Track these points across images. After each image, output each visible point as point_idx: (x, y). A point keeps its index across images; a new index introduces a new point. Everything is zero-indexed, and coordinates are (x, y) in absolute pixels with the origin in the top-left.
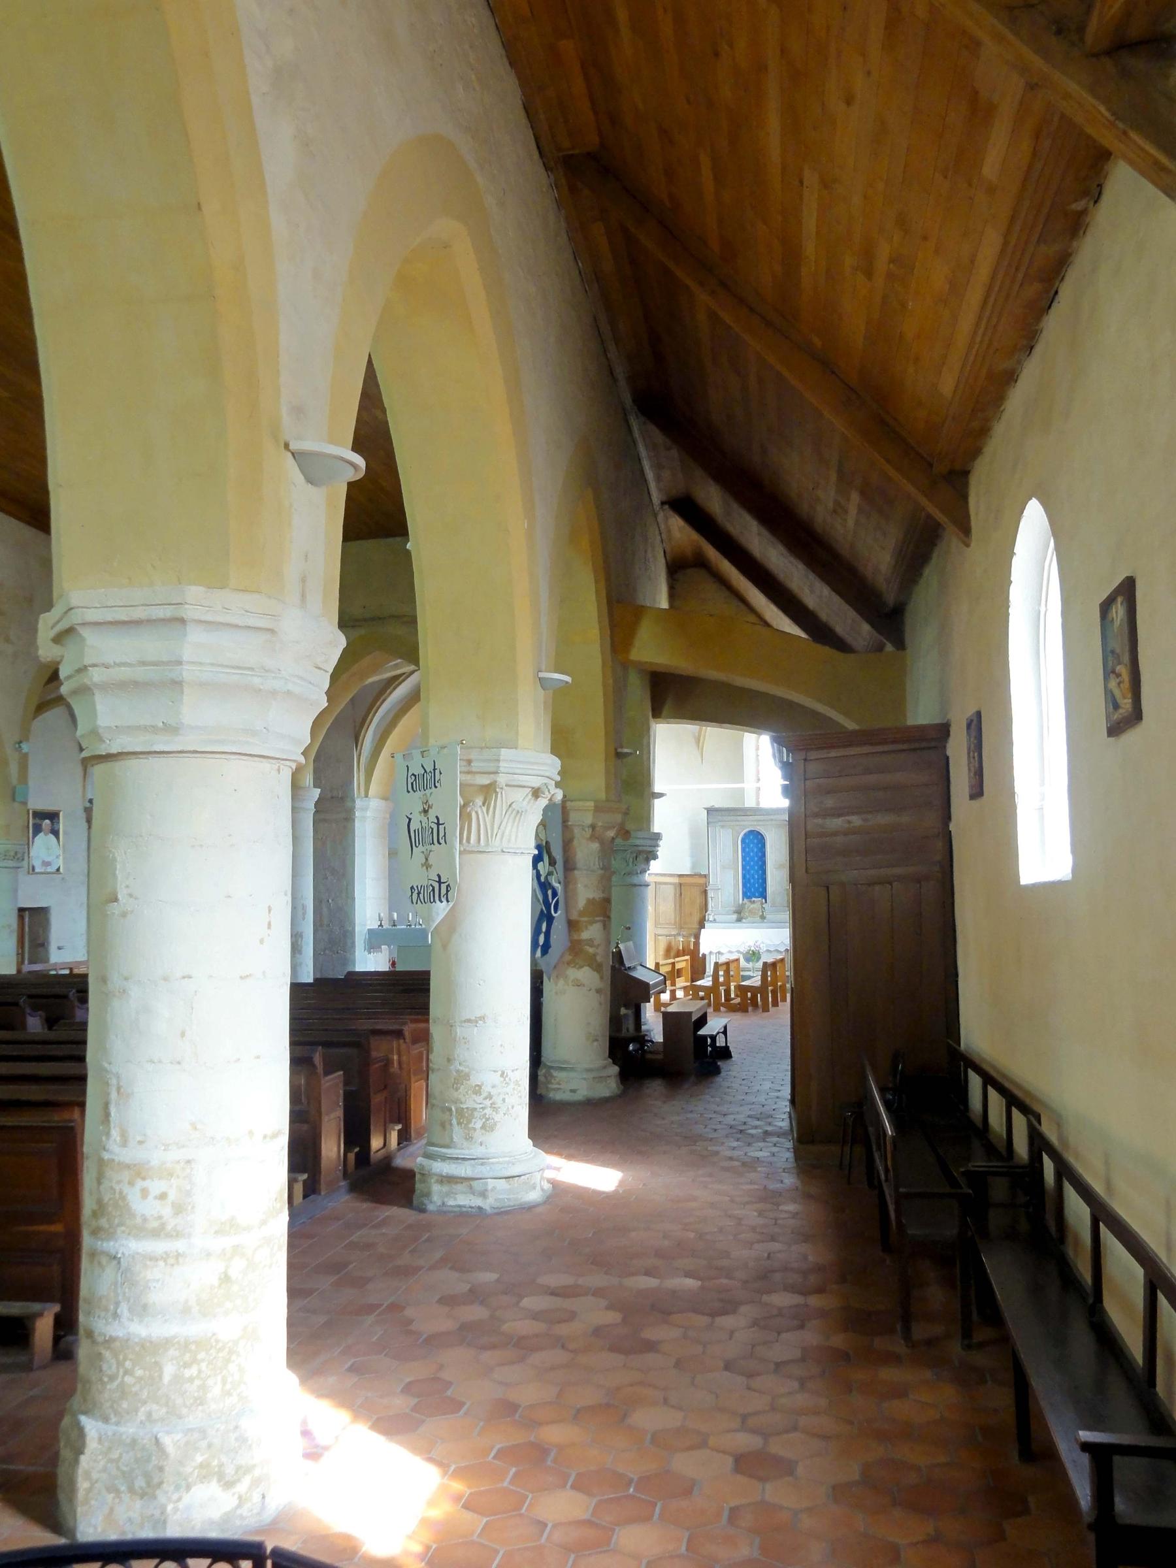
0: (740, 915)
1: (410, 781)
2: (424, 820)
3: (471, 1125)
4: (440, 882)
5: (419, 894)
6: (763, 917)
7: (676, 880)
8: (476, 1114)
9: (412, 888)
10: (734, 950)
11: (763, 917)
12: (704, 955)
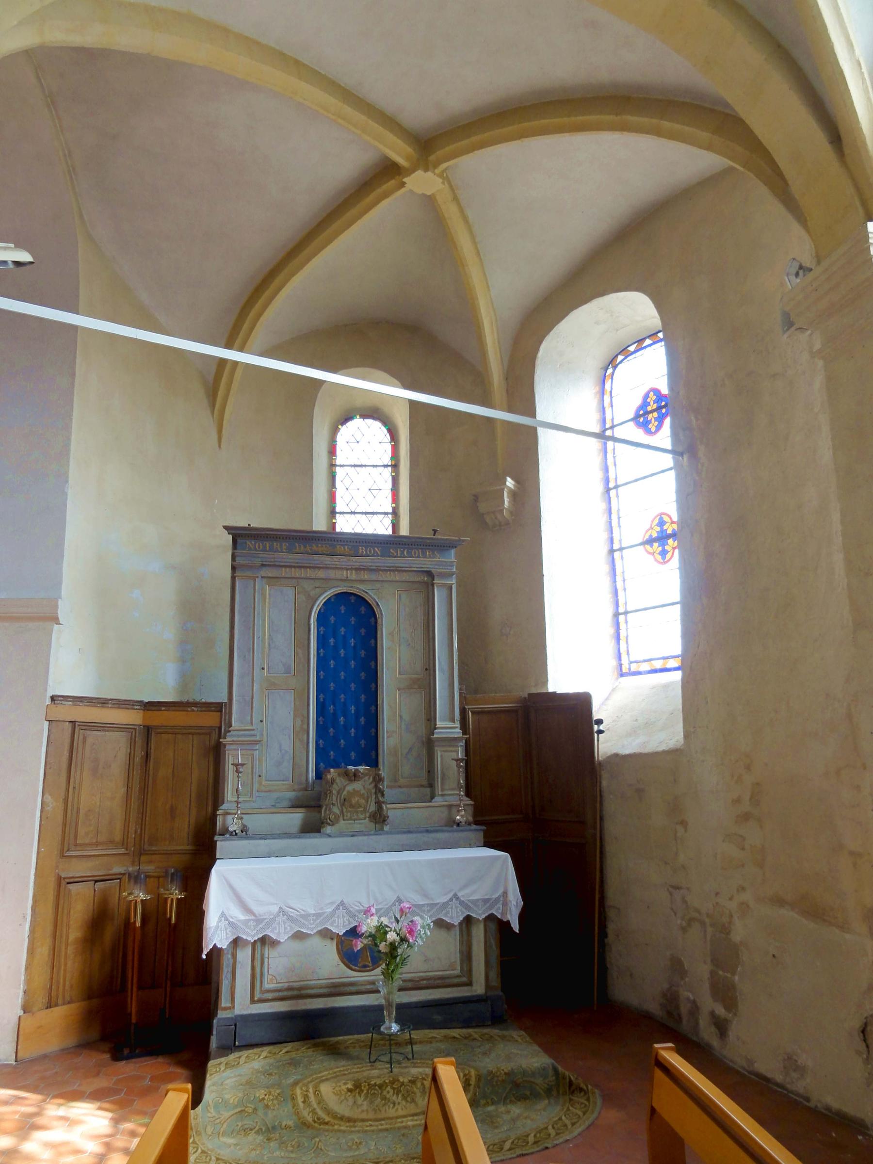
0: (315, 814)
6: (379, 818)
7: (134, 718)
10: (311, 929)
11: (379, 818)
12: (216, 951)
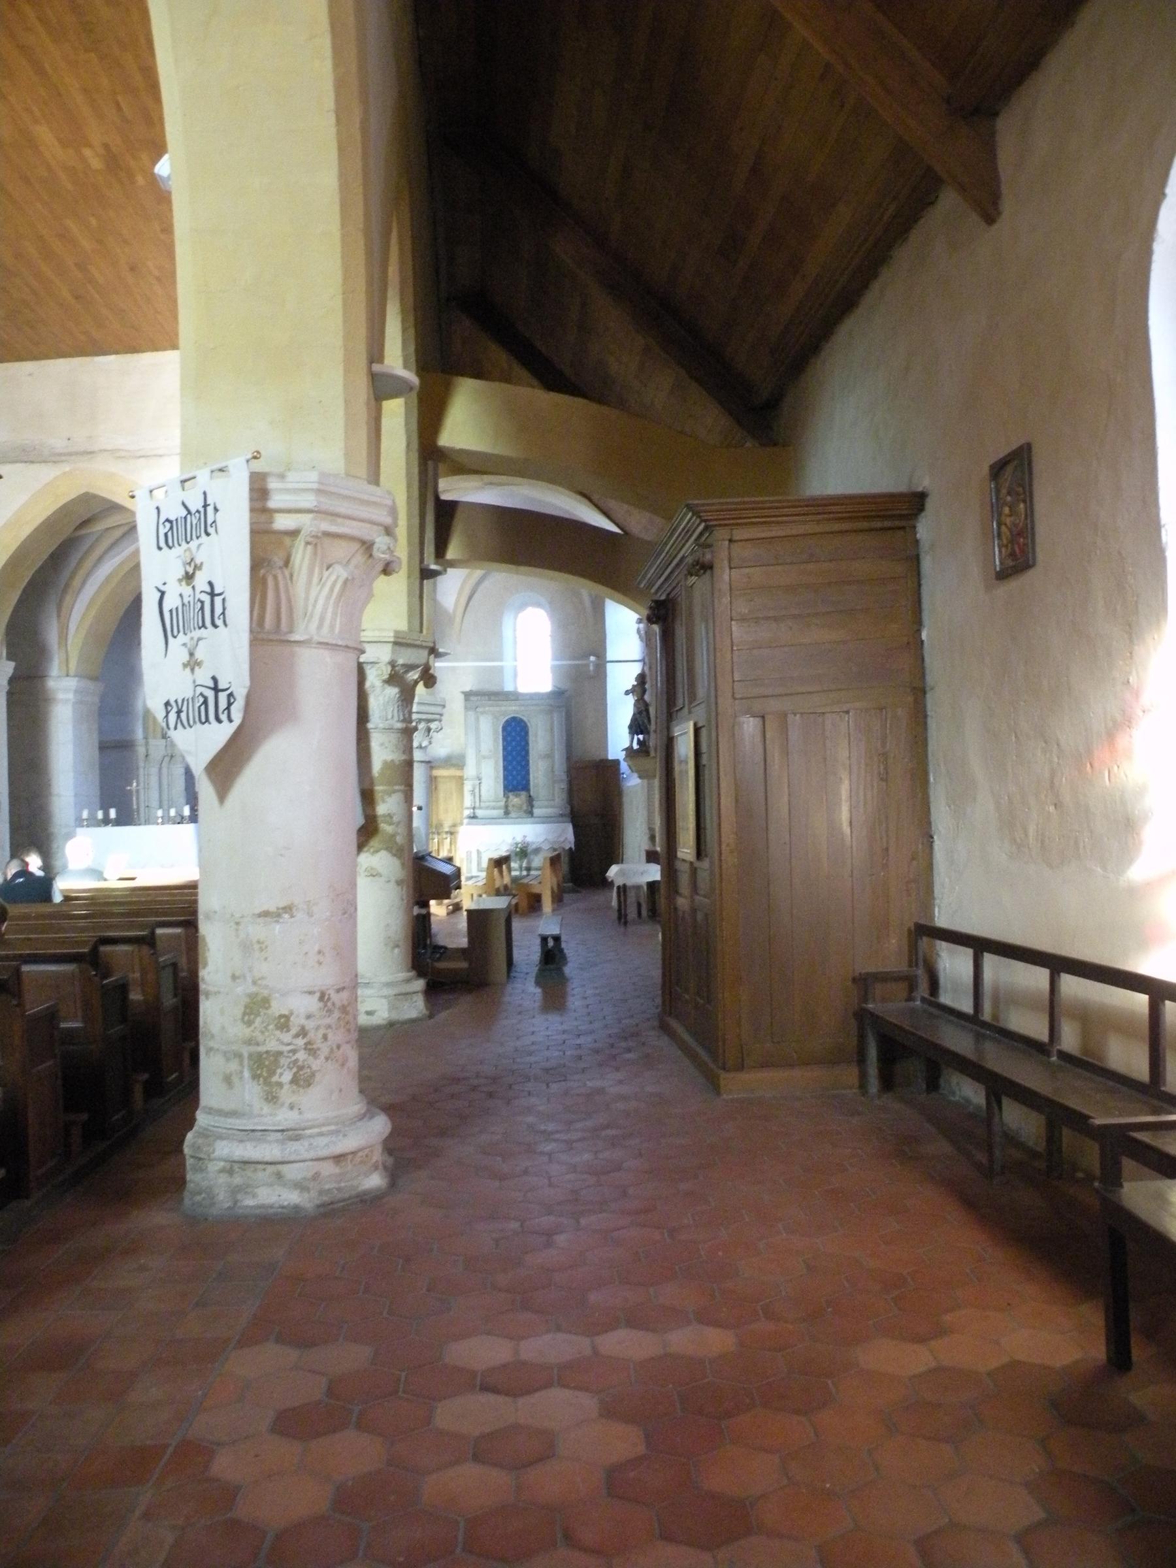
1: (162, 531)
2: (187, 590)
3: (275, 1079)
4: (216, 690)
5: (179, 712)
8: (283, 1061)
9: (167, 704)
